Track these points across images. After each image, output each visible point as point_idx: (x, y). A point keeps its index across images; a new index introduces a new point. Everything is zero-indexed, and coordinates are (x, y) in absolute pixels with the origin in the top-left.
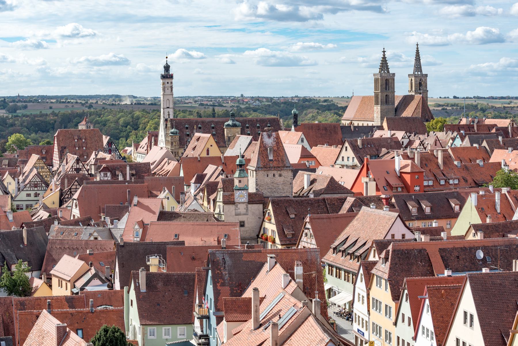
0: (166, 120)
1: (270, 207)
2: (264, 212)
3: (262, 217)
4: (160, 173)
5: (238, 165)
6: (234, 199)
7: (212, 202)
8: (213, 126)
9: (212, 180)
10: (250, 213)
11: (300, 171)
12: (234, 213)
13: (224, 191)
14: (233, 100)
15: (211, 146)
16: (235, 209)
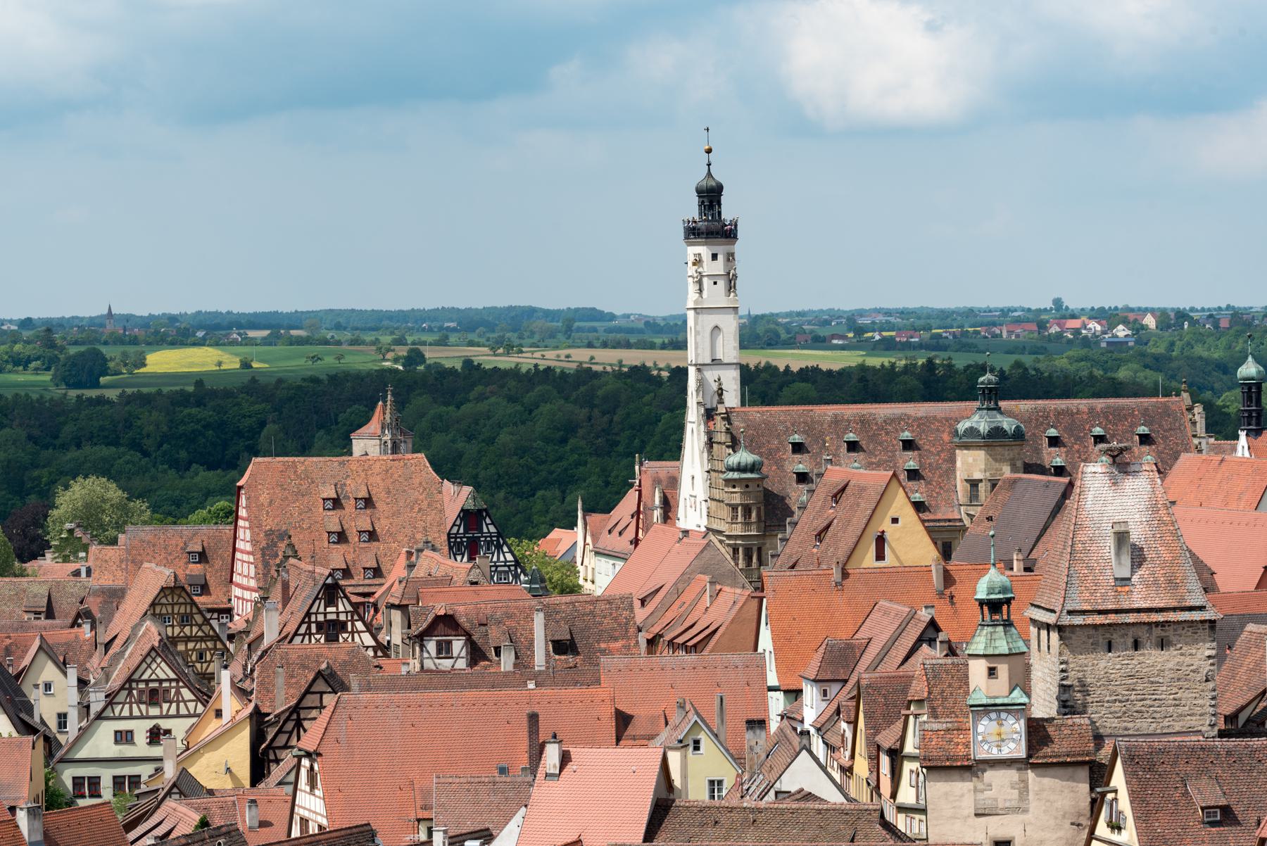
0: (709, 414)
1: (1118, 779)
2: (1093, 801)
3: (1086, 822)
4: (680, 640)
5: (982, 603)
6: (967, 745)
7: (885, 761)
8: (907, 435)
9: (890, 666)
10: (1033, 804)
11: (1251, 627)
12: (968, 806)
13: (934, 714)
14: (1018, 321)
15: (895, 521)
16: (976, 790)
